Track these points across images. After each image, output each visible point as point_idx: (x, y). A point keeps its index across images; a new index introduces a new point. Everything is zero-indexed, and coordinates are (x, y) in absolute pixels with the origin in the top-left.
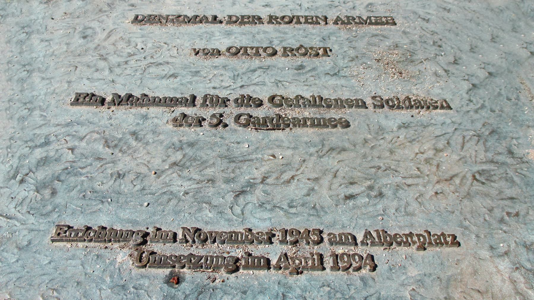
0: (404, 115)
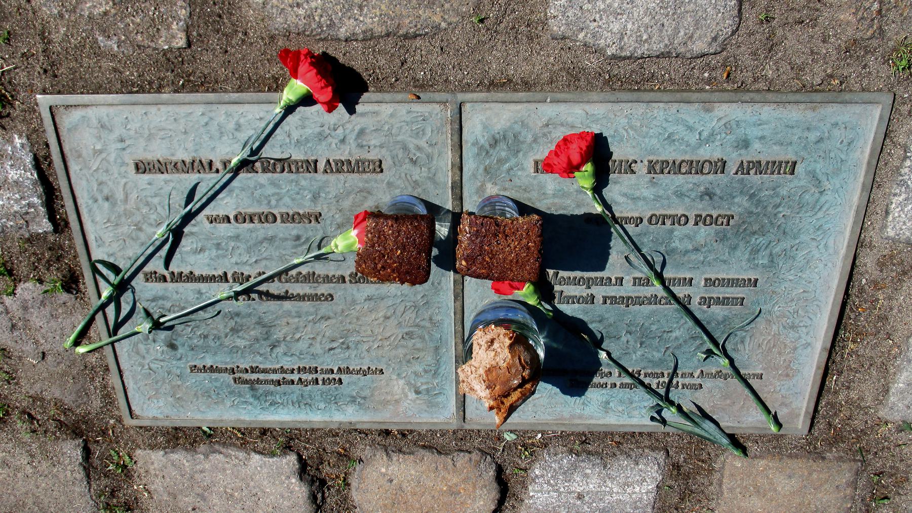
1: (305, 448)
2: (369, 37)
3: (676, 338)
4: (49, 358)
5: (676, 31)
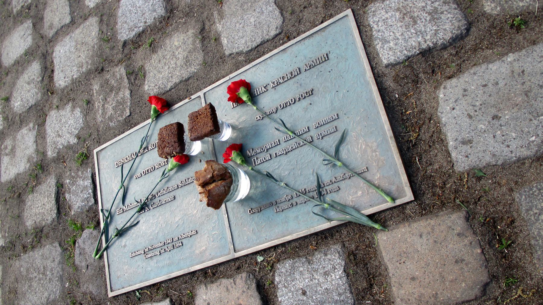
1: (174, 295)
2: (176, 85)
4: (89, 267)
5: (263, 31)
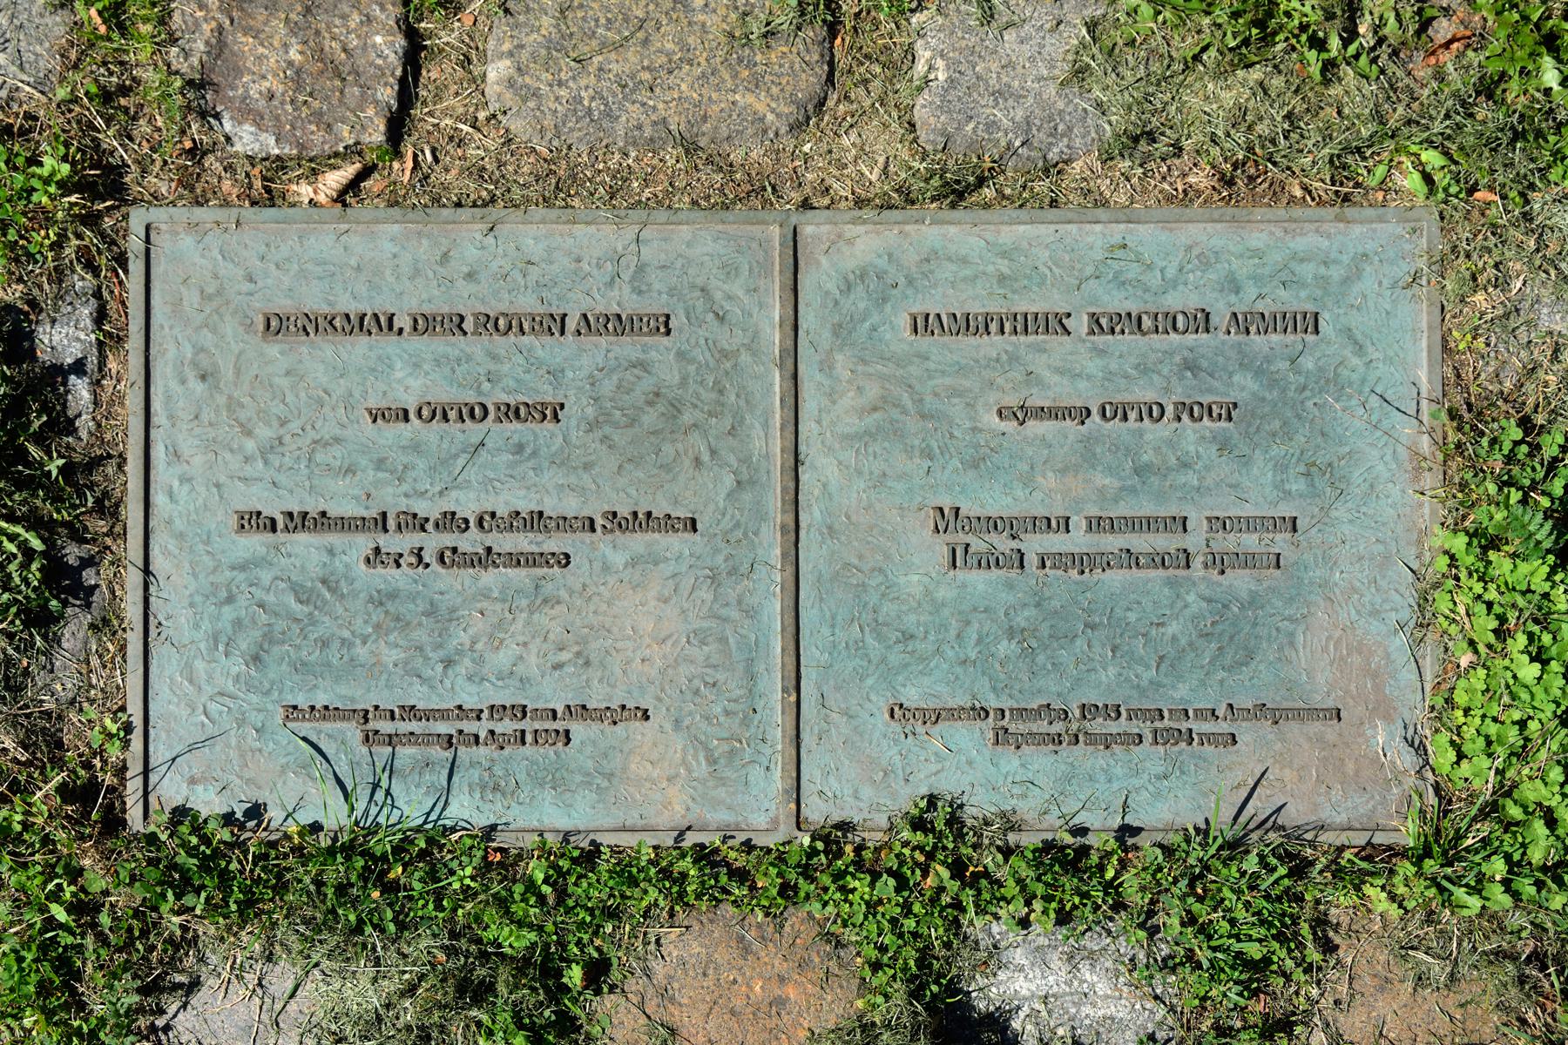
0: (638, 541)
3: (1174, 638)
